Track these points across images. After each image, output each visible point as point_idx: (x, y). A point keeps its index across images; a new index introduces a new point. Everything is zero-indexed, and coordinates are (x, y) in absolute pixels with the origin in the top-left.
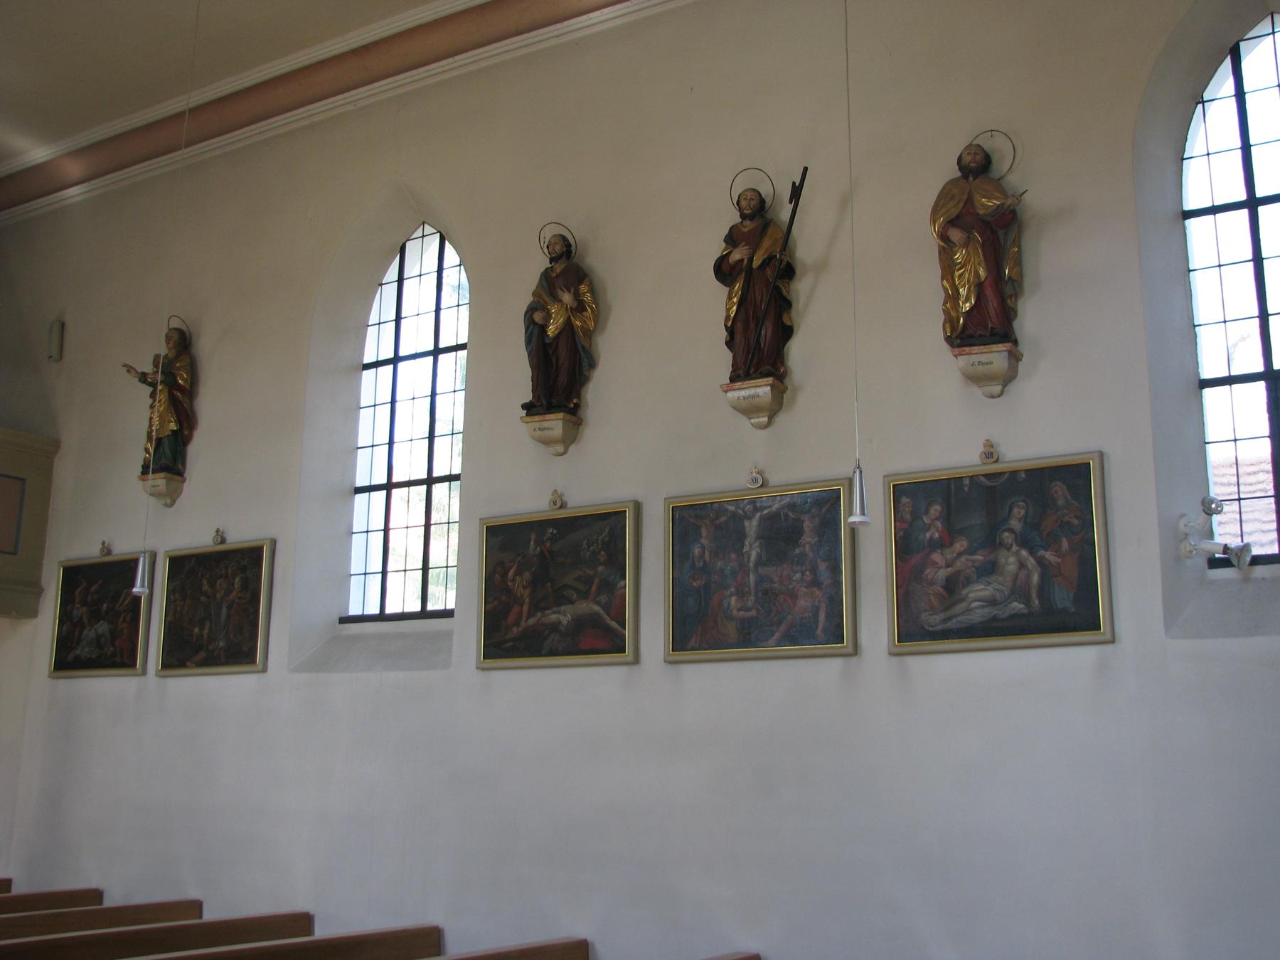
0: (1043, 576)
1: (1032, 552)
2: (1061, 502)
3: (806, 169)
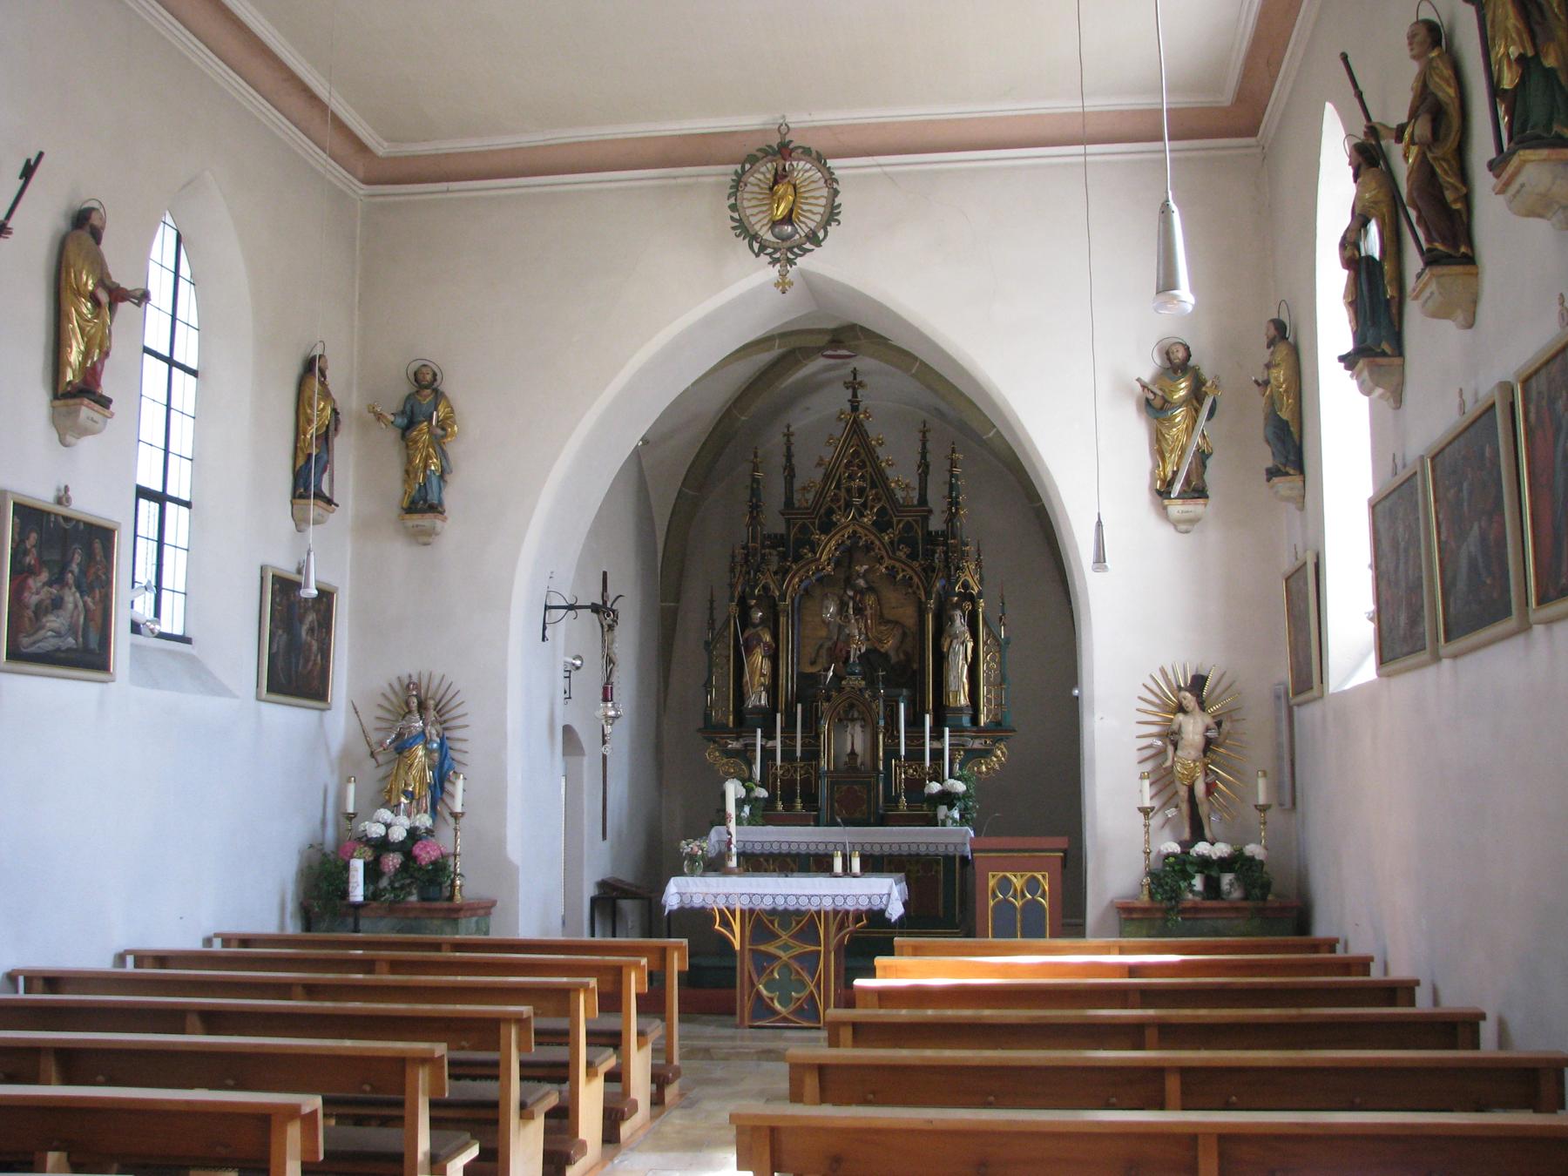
0: (85, 619)
1: (82, 596)
2: (98, 558)
3: (41, 155)
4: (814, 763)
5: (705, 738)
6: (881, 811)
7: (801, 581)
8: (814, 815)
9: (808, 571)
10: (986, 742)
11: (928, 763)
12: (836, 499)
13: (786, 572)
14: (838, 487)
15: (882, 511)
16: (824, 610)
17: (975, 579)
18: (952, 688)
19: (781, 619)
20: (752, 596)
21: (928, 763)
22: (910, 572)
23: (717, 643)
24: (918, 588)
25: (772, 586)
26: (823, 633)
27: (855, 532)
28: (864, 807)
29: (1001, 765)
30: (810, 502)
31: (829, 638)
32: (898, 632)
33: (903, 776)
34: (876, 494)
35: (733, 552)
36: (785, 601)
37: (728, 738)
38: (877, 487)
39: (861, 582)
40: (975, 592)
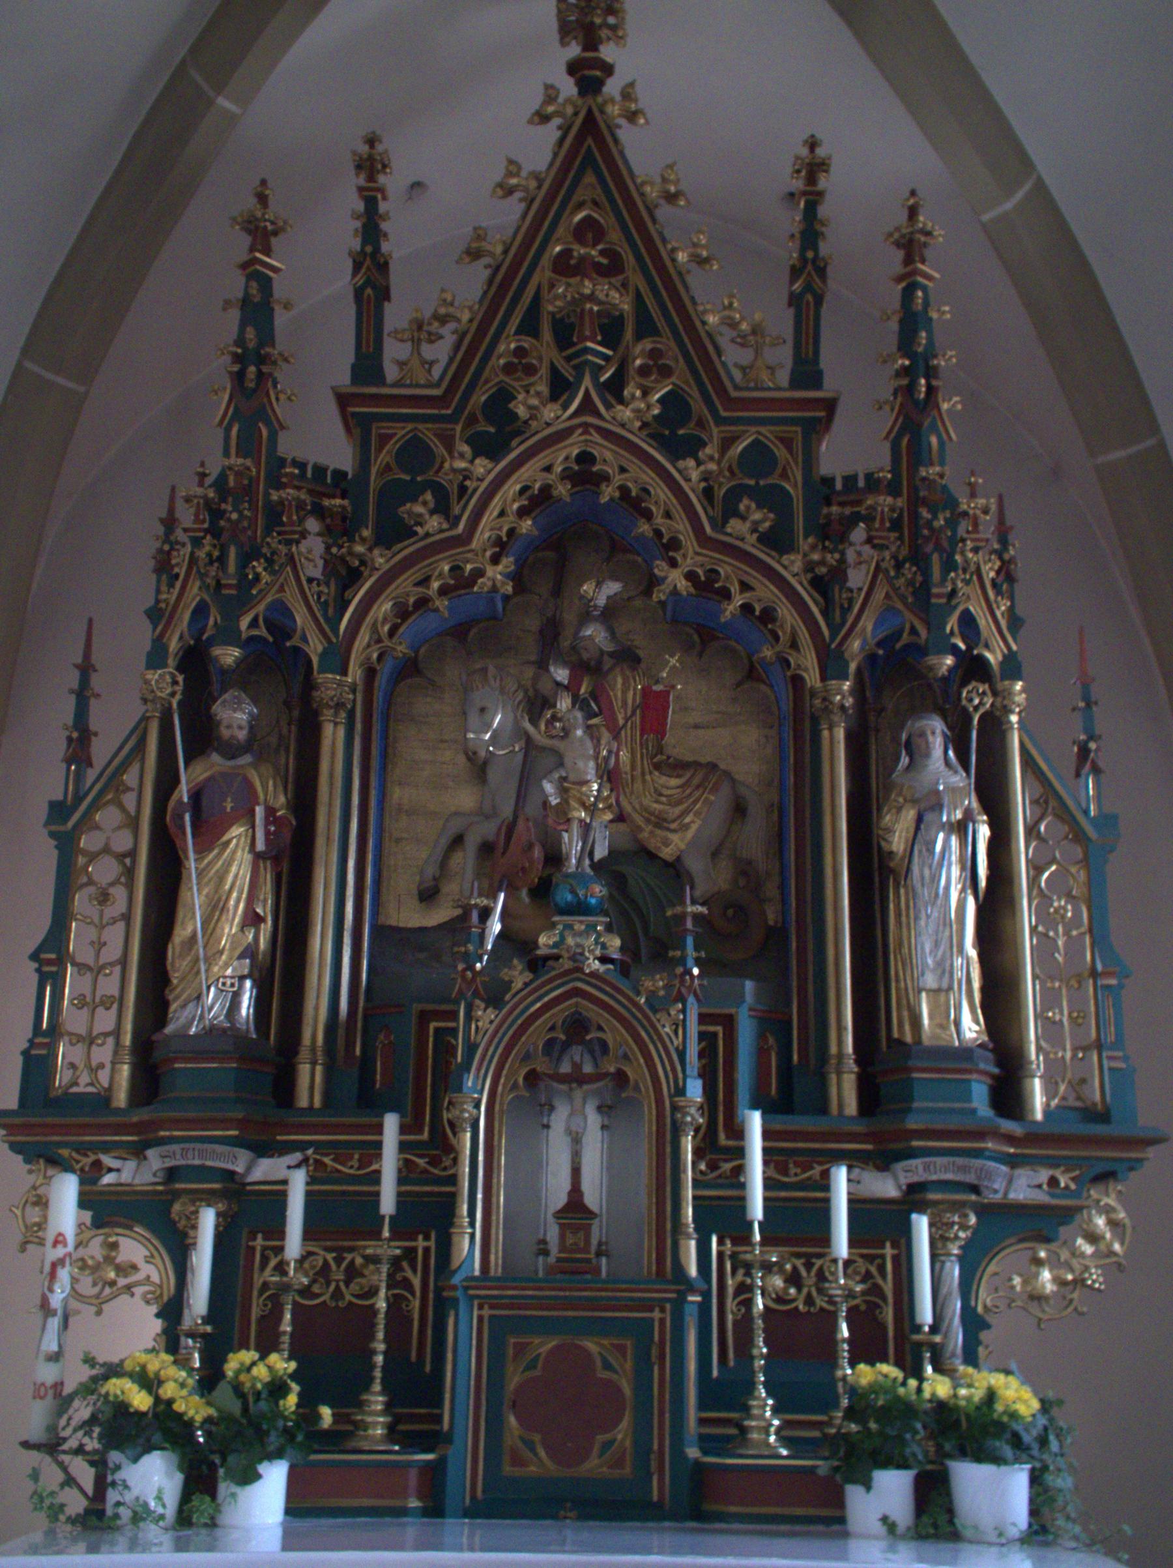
4: (421, 1243)
5: (16, 1148)
6: (693, 1452)
7: (403, 612)
8: (427, 1467)
9: (425, 581)
10: (1053, 1182)
11: (841, 1246)
12: (520, 365)
13: (352, 577)
14: (530, 327)
15: (674, 403)
16: (473, 719)
17: (998, 614)
18: (930, 981)
19: (328, 730)
20: (229, 636)
21: (841, 1246)
22: (765, 593)
23: (95, 806)
24: (794, 645)
25: (301, 618)
26: (466, 799)
27: (585, 458)
28: (623, 1431)
29: (1115, 1267)
30: (437, 372)
31: (484, 814)
32: (720, 800)
33: (760, 1303)
34: (654, 354)
35: (171, 510)
36: (344, 673)
37: (106, 1148)
38: (655, 332)
39: (595, 634)
40: (993, 658)
